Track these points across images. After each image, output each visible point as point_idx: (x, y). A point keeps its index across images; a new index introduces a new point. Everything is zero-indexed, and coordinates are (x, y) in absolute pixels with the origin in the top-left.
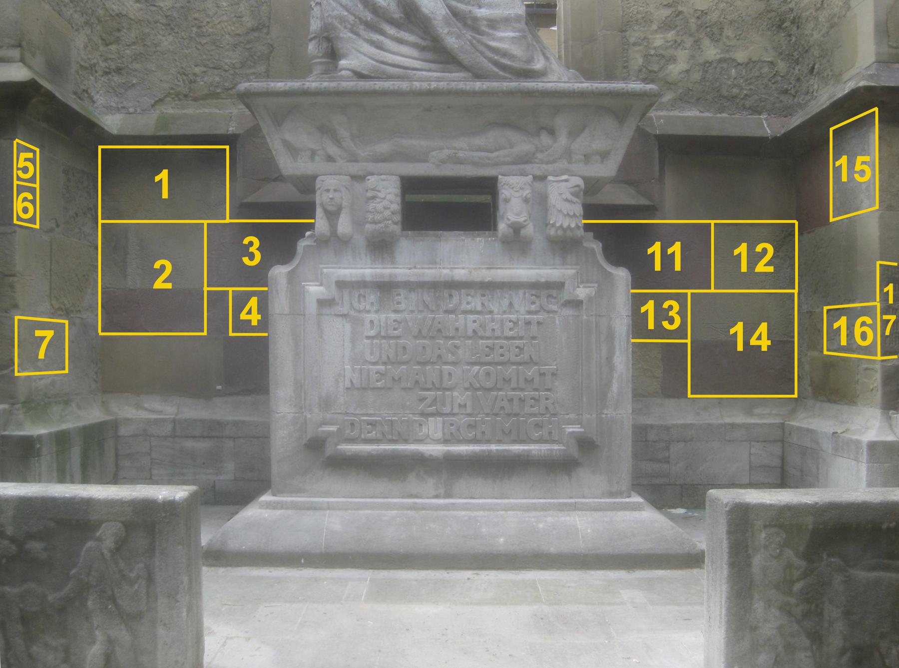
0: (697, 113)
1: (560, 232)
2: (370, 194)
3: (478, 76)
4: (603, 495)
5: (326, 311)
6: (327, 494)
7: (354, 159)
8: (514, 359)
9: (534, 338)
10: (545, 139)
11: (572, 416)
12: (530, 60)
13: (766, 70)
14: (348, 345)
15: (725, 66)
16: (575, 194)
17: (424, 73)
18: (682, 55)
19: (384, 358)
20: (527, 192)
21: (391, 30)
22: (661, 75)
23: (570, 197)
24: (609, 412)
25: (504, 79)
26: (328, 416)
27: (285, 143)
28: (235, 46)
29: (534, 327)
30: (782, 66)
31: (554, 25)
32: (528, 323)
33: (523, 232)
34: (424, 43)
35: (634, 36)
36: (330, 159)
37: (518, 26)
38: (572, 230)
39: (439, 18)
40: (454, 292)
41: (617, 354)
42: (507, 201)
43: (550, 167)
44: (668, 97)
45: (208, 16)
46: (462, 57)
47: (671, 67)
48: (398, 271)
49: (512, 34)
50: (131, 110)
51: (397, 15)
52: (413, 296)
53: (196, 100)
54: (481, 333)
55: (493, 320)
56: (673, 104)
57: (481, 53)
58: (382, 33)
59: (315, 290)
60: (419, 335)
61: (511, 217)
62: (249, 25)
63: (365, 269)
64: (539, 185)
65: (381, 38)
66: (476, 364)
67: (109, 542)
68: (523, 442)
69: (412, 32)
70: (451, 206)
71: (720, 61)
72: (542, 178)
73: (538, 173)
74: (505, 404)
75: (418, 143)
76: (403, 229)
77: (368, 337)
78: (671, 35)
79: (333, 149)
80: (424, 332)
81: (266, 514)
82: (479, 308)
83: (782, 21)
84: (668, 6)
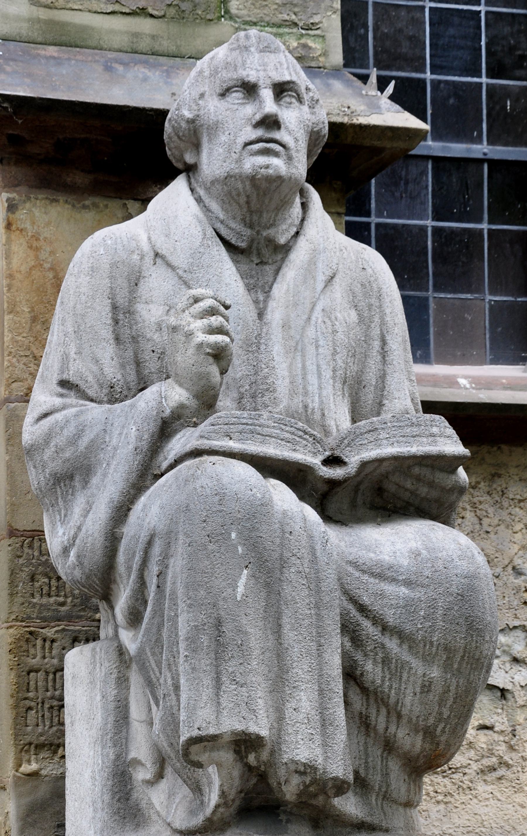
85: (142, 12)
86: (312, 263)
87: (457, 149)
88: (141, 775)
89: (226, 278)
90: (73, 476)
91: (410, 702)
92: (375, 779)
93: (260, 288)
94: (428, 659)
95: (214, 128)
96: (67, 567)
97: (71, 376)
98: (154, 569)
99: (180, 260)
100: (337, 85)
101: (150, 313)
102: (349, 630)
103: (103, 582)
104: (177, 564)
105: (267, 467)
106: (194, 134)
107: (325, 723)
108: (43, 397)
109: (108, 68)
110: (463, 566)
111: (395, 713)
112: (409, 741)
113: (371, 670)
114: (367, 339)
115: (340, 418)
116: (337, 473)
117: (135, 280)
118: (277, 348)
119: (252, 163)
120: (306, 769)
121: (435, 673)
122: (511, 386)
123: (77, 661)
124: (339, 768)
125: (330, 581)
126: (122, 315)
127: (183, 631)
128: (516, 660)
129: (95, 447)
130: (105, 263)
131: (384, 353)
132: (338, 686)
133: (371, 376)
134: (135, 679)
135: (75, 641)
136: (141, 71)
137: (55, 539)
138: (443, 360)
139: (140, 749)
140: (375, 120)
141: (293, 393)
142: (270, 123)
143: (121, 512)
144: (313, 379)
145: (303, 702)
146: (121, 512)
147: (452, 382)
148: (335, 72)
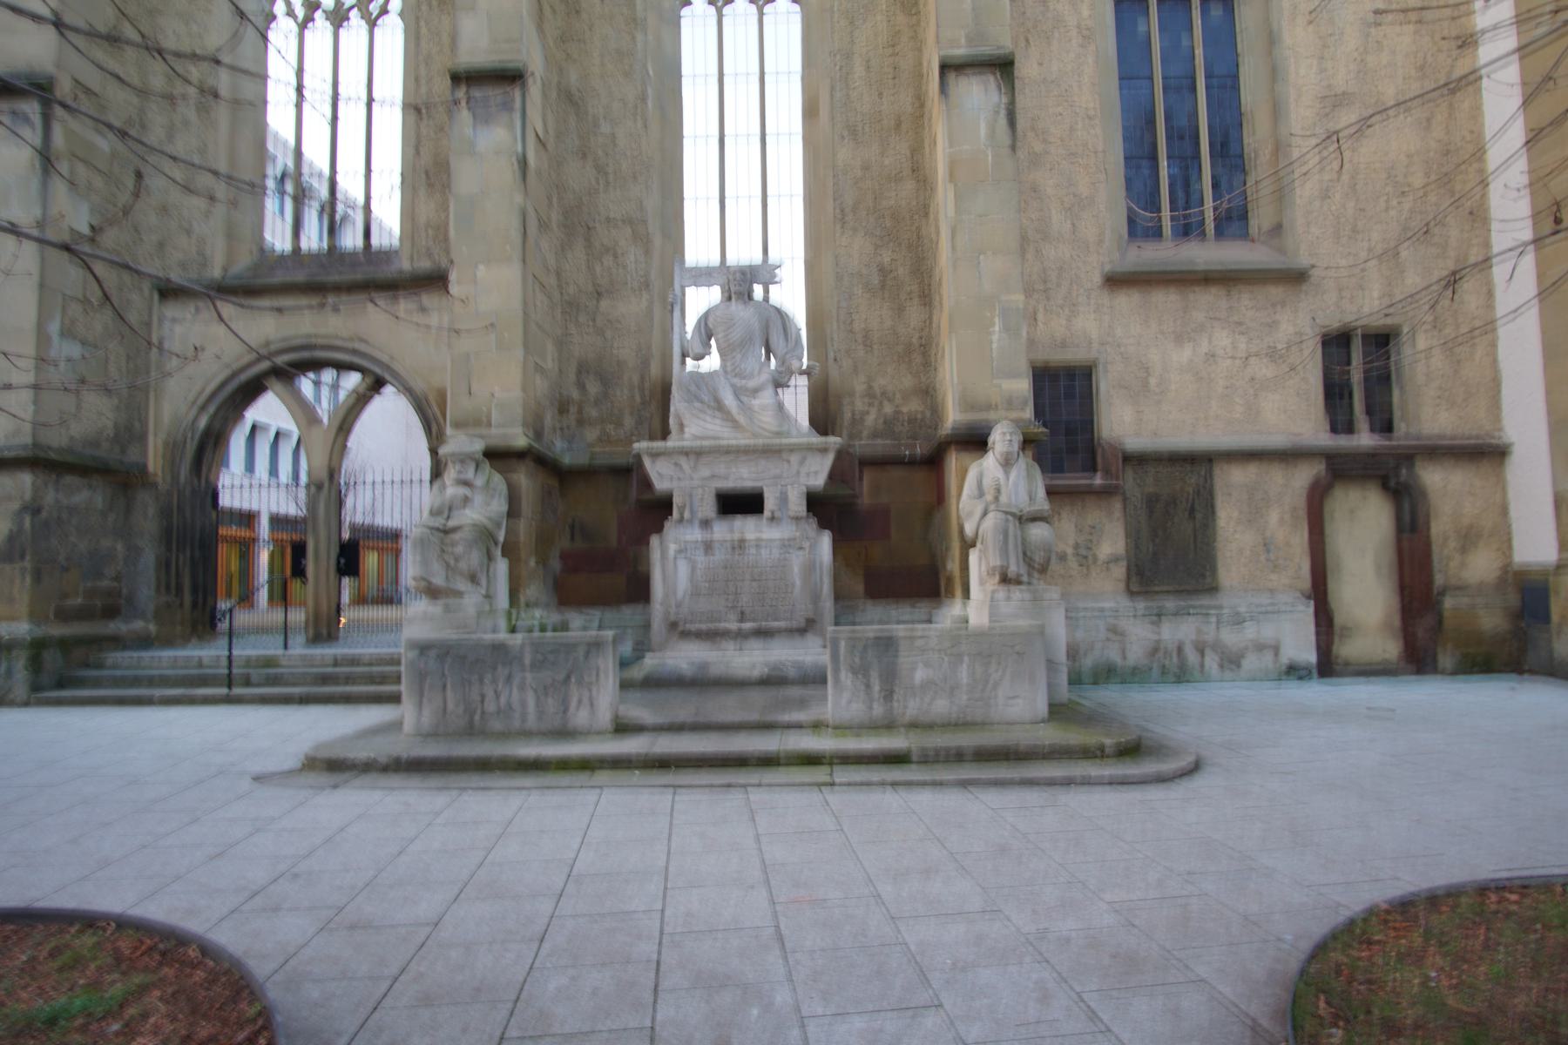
59: (672, 548)
63: (695, 534)
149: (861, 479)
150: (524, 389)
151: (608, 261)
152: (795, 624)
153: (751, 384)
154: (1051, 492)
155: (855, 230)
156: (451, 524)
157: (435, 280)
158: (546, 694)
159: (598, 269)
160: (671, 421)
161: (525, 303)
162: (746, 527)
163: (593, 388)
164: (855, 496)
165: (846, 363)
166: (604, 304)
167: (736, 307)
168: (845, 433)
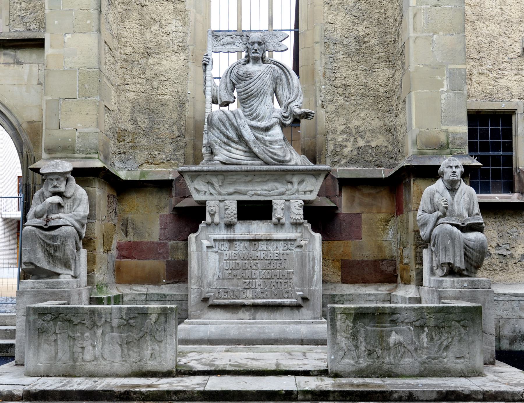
0: (356, 168)
1: (295, 221)
2: (226, 207)
3: (266, 163)
4: (311, 319)
5: (210, 250)
6: (209, 319)
7: (220, 194)
8: (278, 268)
9: (285, 260)
10: (290, 186)
11: (300, 289)
12: (284, 156)
13: (383, 149)
14: (218, 263)
15: (367, 148)
16: (301, 207)
17: (246, 161)
18: (349, 145)
19: (231, 268)
20: (283, 206)
21: (233, 145)
22: (340, 153)
23: (298, 208)
24: (313, 287)
25: (275, 164)
26: (210, 289)
27: (195, 189)
28: (171, 143)
29: (286, 256)
30: (390, 148)
31: (300, 130)
32: (284, 254)
33: (281, 220)
34: (246, 150)
35: (329, 137)
36: (211, 194)
37: (280, 143)
38: (299, 220)
39: (251, 141)
40: (256, 243)
41: (316, 265)
42: (275, 209)
43: (291, 197)
44: (343, 162)
45: (160, 131)
46: (259, 155)
47: (345, 149)
48: (236, 236)
49: (278, 147)
50: (130, 169)
51: (236, 139)
52: (242, 245)
53: (156, 165)
54: (266, 258)
55: (270, 253)
56: (346, 165)
57: (267, 154)
58: (230, 146)
60: (244, 259)
61: (278, 216)
62: (177, 135)
63: (223, 234)
64: (287, 203)
65: (230, 148)
66: (264, 269)
67: (153, 320)
68: (281, 298)
69: (241, 145)
70: (255, 211)
71: (365, 146)
72: (289, 200)
73: (287, 199)
74: (275, 284)
75: (242, 188)
76: (238, 220)
77: (225, 260)
78: (345, 136)
79: (212, 191)
80: (245, 258)
81: (187, 326)
82: (265, 249)
83: (391, 129)
84: (344, 124)
85: (435, 149)
86: (461, 191)
87: (496, 153)
88: (435, 268)
89: (448, 195)
90: (424, 224)
91: (474, 258)
92: (469, 269)
93: (453, 196)
94: (476, 252)
95: (446, 173)
96: (423, 238)
97: (424, 209)
98: (436, 239)
99: (441, 192)
100: (467, 158)
101: (436, 200)
102: (465, 248)
103: (429, 240)
104: (440, 239)
105: (453, 225)
106: (443, 173)
107: (461, 261)
108: (419, 212)
109: (429, 159)
110: (482, 239)
111: (472, 260)
112: (475, 264)
113: (468, 254)
114: (471, 202)
115: (466, 215)
116: (464, 225)
117: (434, 195)
118: (455, 205)
119: (451, 178)
120: (458, 267)
121: (478, 254)
122: (507, 198)
123: (425, 251)
124: (463, 267)
125: (462, 241)
126: (432, 200)
127: (441, 248)
128: (507, 250)
129: (428, 221)
130: (429, 192)
131: (473, 204)
132: (463, 256)
133: (471, 208)
134: (434, 254)
135: (424, 248)
136: (435, 158)
137: (422, 233)
138: (493, 193)
139: (435, 264)
140: (473, 164)
141: (458, 211)
142: (454, 172)
143: (432, 231)
144: (461, 209)
145: (458, 258)
146: (432, 231)
147: (494, 198)
148: (467, 155)
149: (340, 195)
150: (98, 126)
151: (155, 28)
152: (293, 301)
153: (263, 124)
154: (483, 206)
155: (339, 11)
156: (51, 224)
157: (38, 44)
158: (129, 349)
159: (148, 36)
160: (204, 150)
161: (100, 63)
162: (258, 229)
163: (143, 121)
164: (336, 208)
165: (331, 108)
166: (151, 60)
167: (251, 67)
168: (328, 160)
